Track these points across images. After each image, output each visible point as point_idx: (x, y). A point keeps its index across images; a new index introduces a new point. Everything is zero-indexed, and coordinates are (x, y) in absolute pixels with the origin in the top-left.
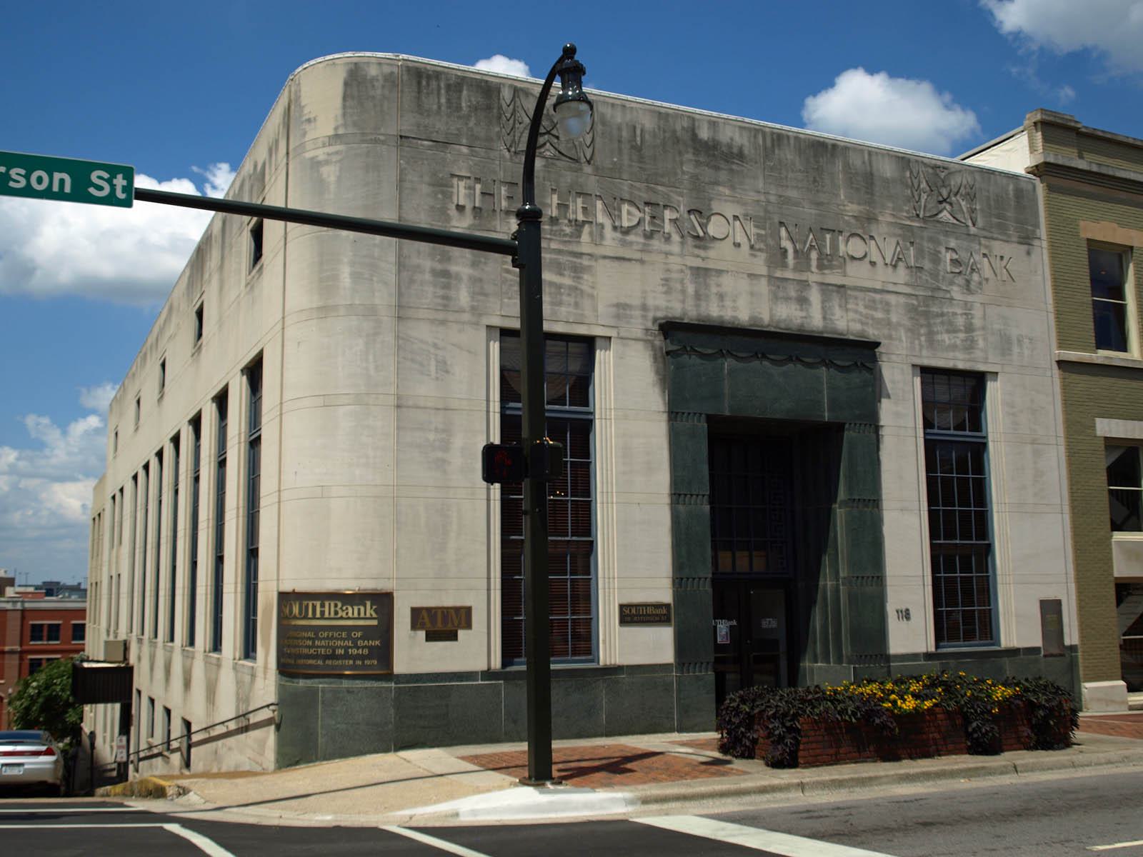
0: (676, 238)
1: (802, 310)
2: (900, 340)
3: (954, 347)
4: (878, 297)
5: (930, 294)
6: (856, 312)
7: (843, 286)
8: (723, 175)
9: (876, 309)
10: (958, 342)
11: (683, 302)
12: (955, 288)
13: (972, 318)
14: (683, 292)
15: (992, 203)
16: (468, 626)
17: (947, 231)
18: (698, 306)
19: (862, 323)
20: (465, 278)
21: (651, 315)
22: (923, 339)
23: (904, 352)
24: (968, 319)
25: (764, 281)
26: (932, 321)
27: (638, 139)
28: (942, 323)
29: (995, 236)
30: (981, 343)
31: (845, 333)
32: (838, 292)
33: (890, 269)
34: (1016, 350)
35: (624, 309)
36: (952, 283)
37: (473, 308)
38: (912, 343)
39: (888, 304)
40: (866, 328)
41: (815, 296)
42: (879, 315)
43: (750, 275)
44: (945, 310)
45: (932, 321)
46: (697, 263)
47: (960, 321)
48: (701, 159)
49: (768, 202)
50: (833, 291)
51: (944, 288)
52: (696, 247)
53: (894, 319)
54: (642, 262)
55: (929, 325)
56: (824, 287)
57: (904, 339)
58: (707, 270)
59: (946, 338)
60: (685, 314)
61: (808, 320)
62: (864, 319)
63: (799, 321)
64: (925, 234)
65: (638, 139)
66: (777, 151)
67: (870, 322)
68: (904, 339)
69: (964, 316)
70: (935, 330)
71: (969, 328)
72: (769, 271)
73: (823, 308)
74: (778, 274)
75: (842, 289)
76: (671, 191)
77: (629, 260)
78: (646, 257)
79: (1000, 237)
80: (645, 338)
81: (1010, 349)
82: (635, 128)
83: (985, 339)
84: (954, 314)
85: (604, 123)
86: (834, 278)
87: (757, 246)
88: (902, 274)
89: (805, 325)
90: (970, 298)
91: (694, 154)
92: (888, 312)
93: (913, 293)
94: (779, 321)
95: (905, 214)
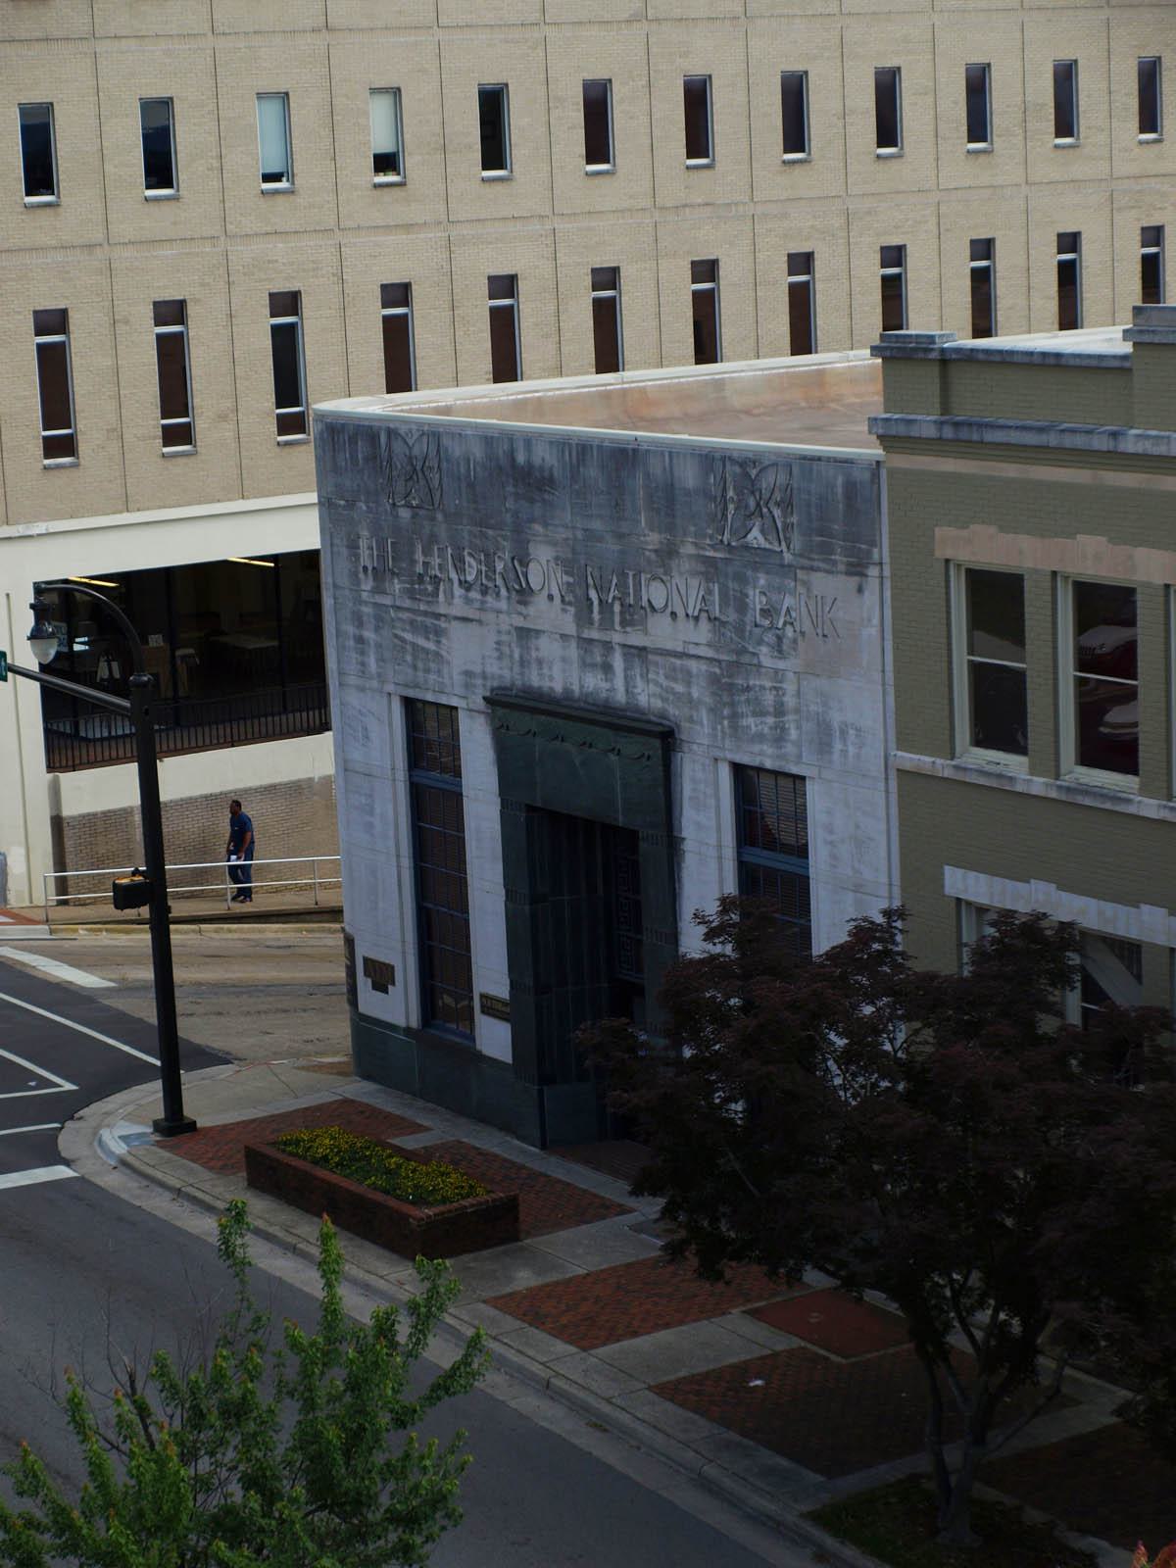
0: (504, 592)
1: (606, 680)
2: (702, 725)
3: (760, 738)
4: (678, 662)
5: (734, 658)
6: (657, 683)
7: (644, 649)
8: (538, 509)
9: (675, 680)
10: (766, 730)
11: (511, 669)
12: (764, 649)
13: (784, 695)
14: (511, 656)
15: (813, 511)
16: (393, 984)
17: (756, 562)
18: (522, 674)
19: (664, 700)
20: (372, 643)
21: (489, 684)
22: (726, 722)
23: (706, 741)
24: (778, 695)
25: (574, 644)
26: (737, 698)
27: (472, 473)
28: (748, 701)
29: (816, 564)
30: (793, 734)
31: (646, 712)
32: (639, 656)
33: (692, 622)
34: (838, 746)
35: (470, 677)
36: (760, 642)
37: (379, 675)
38: (714, 729)
39: (689, 673)
40: (666, 706)
41: (618, 662)
42: (679, 688)
43: (562, 636)
44: (751, 683)
45: (737, 698)
46: (519, 622)
47: (769, 699)
48: (520, 491)
49: (575, 539)
50: (633, 655)
51: (751, 650)
52: (519, 602)
53: (695, 695)
54: (480, 622)
55: (733, 705)
56: (626, 650)
57: (705, 722)
58: (529, 630)
59: (750, 721)
60: (513, 684)
61: (612, 694)
62: (664, 694)
63: (604, 695)
64: (730, 570)
65: (472, 473)
66: (581, 469)
67: (671, 698)
68: (705, 722)
69: (774, 692)
70: (740, 710)
71: (780, 711)
72: (577, 631)
73: (626, 677)
74: (586, 634)
75: (644, 653)
76: (499, 535)
77: (471, 620)
78: (484, 617)
79: (822, 565)
80: (486, 710)
81: (830, 745)
82: (469, 460)
83: (799, 728)
84: (762, 688)
85: (448, 461)
86: (636, 639)
87: (567, 599)
88: (703, 632)
89: (611, 700)
90: (781, 665)
91: (514, 486)
92: (689, 684)
93: (716, 657)
94: (587, 695)
95: (708, 541)
